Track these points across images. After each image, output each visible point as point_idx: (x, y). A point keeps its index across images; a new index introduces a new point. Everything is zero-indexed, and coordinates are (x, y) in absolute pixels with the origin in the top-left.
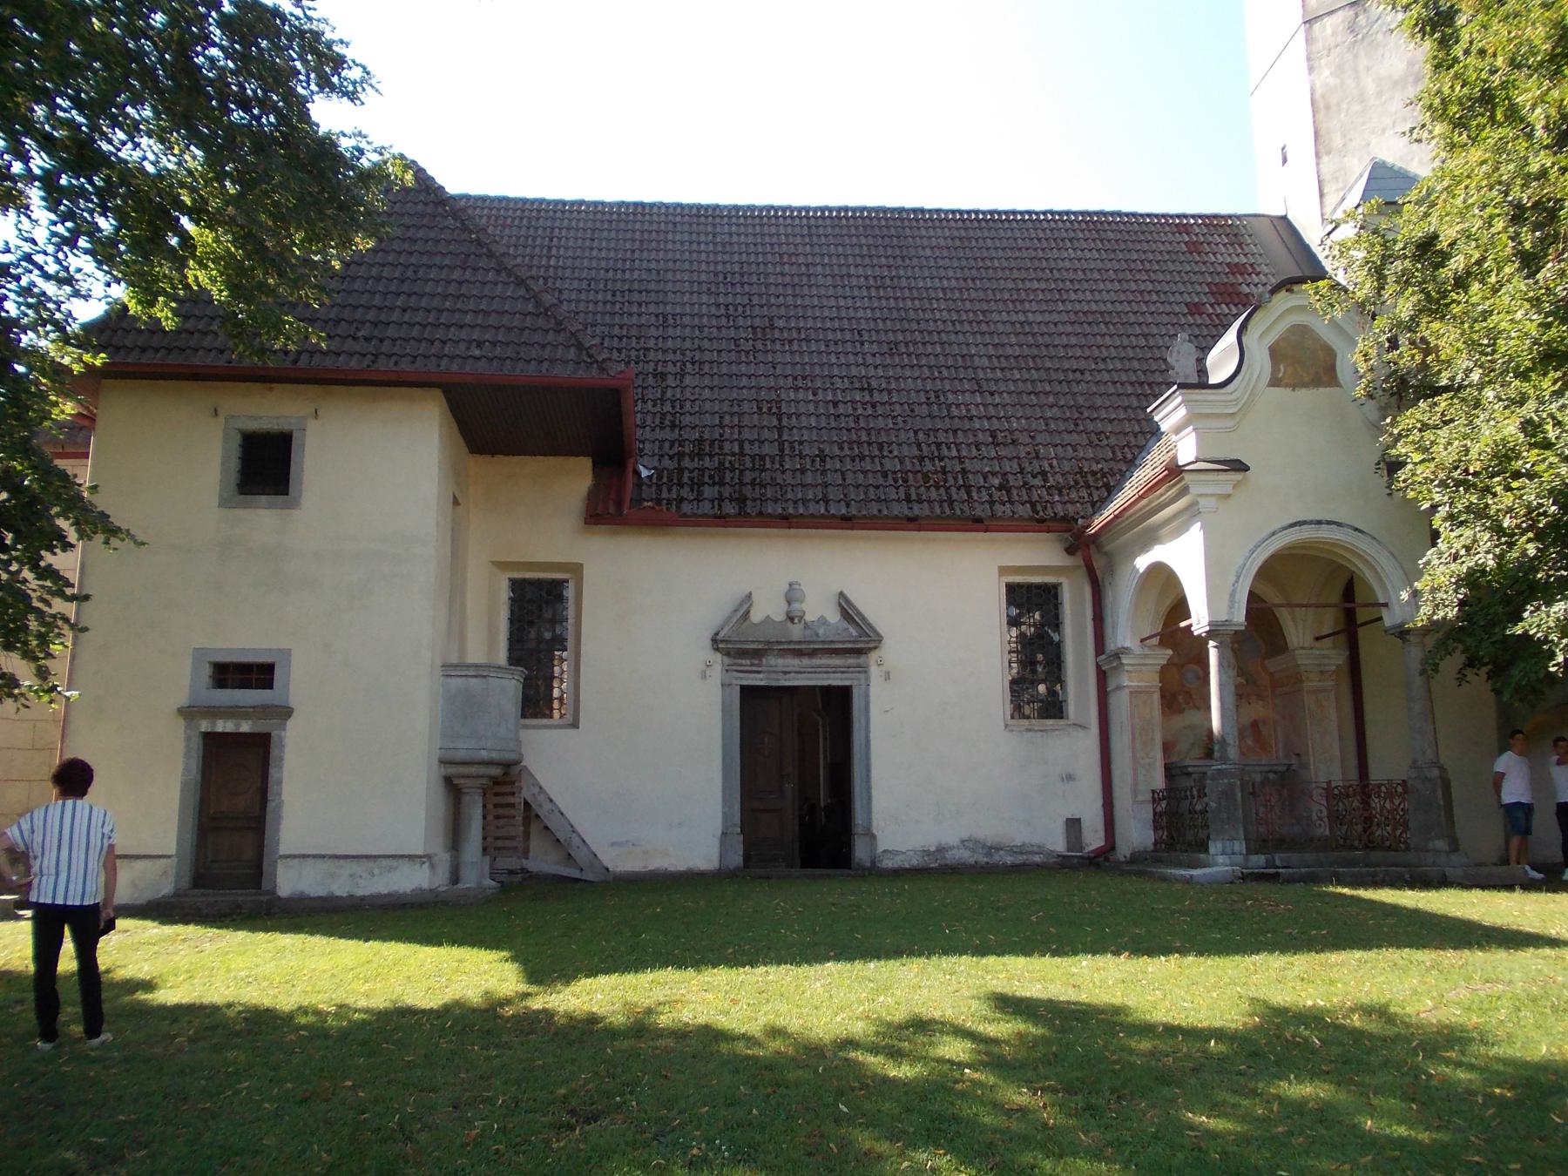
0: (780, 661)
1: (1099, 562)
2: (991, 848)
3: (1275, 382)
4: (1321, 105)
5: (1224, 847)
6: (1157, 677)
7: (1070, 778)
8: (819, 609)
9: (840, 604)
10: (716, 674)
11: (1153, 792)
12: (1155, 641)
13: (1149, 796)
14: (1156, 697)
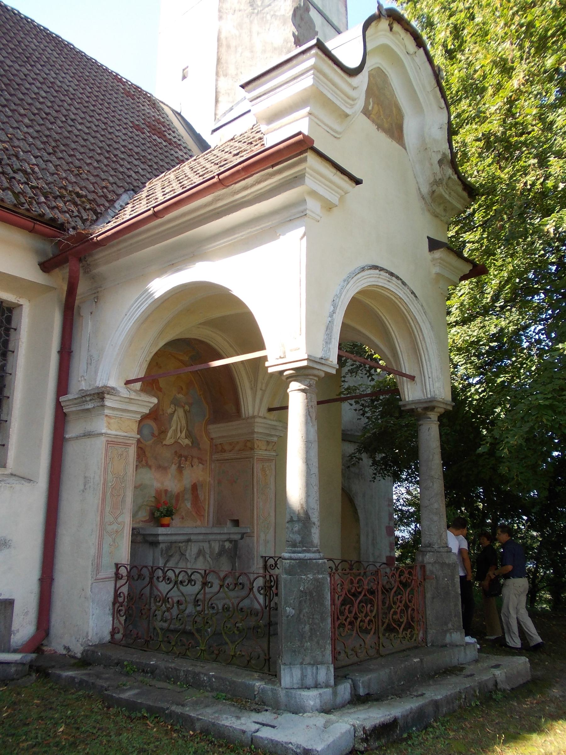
1: (82, 288)
4: (224, 42)
5: (303, 677)
6: (135, 427)
11: (117, 566)
12: (138, 385)
13: (111, 572)
14: (132, 451)
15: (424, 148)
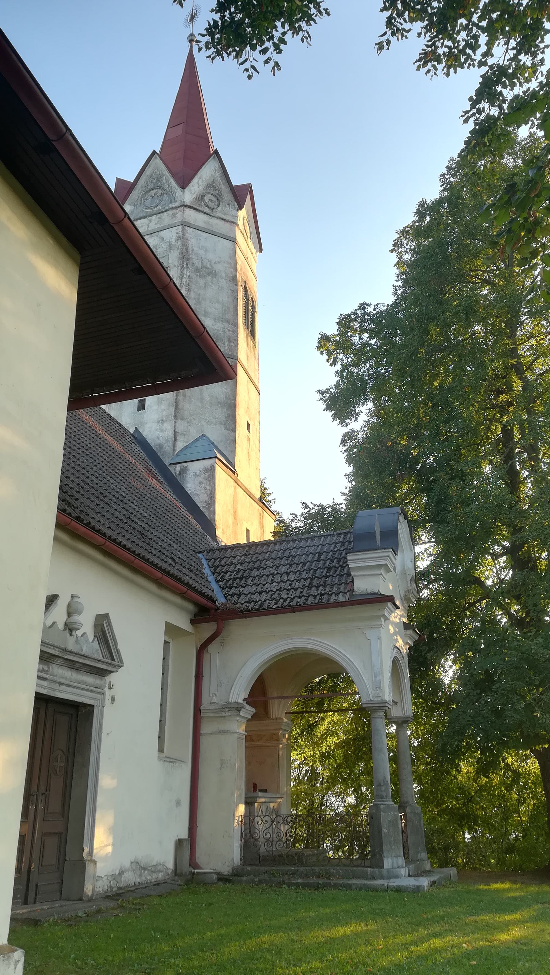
5: (393, 863)
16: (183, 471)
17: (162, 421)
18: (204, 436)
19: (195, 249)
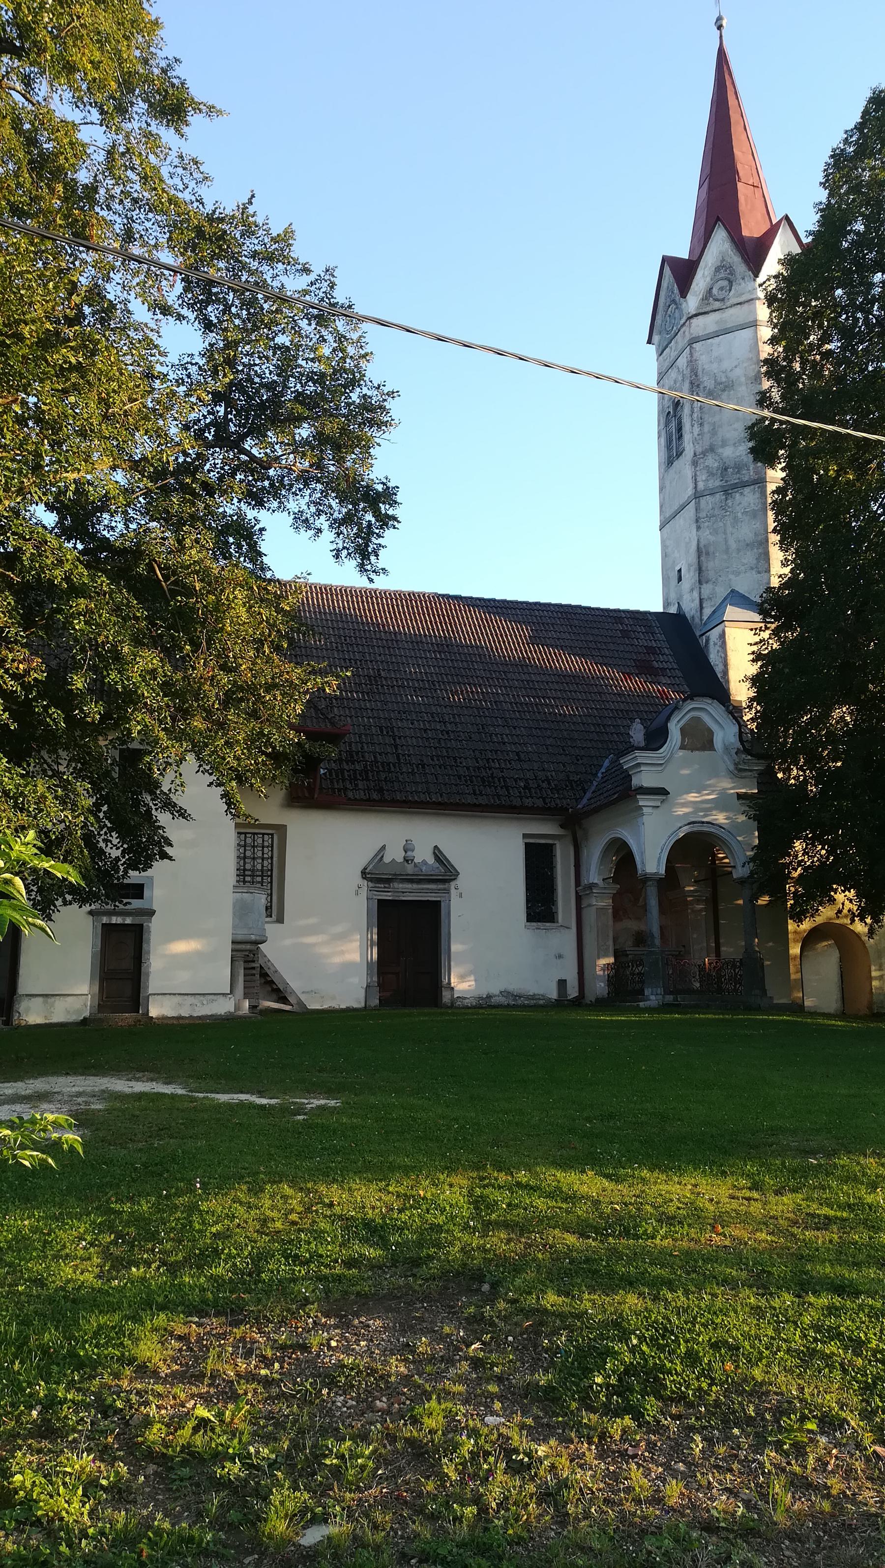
0: (401, 885)
1: (579, 834)
2: (516, 996)
3: (682, 747)
7: (560, 956)
8: (423, 855)
9: (434, 853)
10: (364, 893)
14: (610, 911)
15: (726, 749)
16: (708, 641)
17: (692, 590)
18: (733, 591)
19: (706, 367)
